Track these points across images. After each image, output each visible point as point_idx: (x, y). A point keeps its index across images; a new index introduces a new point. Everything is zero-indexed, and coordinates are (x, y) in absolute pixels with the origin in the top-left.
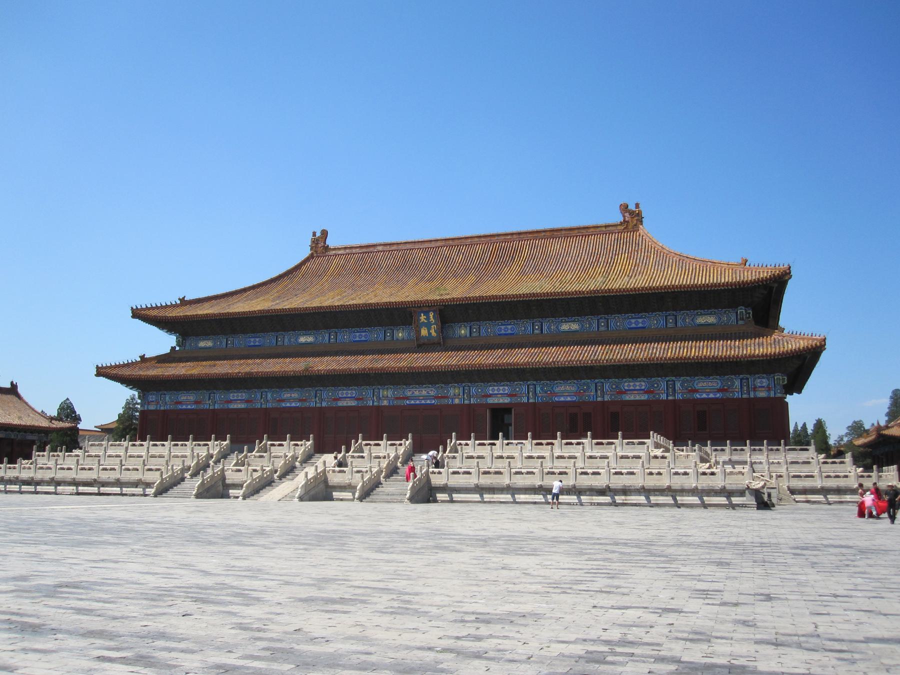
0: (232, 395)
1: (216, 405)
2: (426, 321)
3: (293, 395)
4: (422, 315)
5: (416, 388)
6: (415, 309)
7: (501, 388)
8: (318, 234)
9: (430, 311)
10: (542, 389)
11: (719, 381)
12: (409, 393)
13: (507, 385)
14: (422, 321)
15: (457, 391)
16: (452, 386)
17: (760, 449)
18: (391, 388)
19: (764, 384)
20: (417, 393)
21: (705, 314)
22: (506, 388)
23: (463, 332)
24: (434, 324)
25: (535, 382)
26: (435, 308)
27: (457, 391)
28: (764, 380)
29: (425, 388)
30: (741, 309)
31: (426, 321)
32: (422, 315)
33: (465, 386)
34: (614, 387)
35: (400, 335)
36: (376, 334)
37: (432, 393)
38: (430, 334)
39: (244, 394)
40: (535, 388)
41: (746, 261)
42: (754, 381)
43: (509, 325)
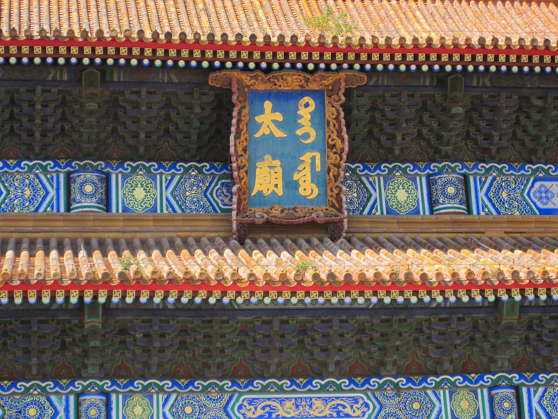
2: (279, 134)
4: (268, 105)
5: (281, 390)
6: (245, 77)
9: (302, 93)
14: (264, 131)
16: (438, 386)
18: (161, 389)
23: (401, 195)
24: (312, 147)
26: (330, 79)
27: (464, 404)
29: (323, 389)
31: (279, 134)
35: (139, 193)
36: (31, 185)
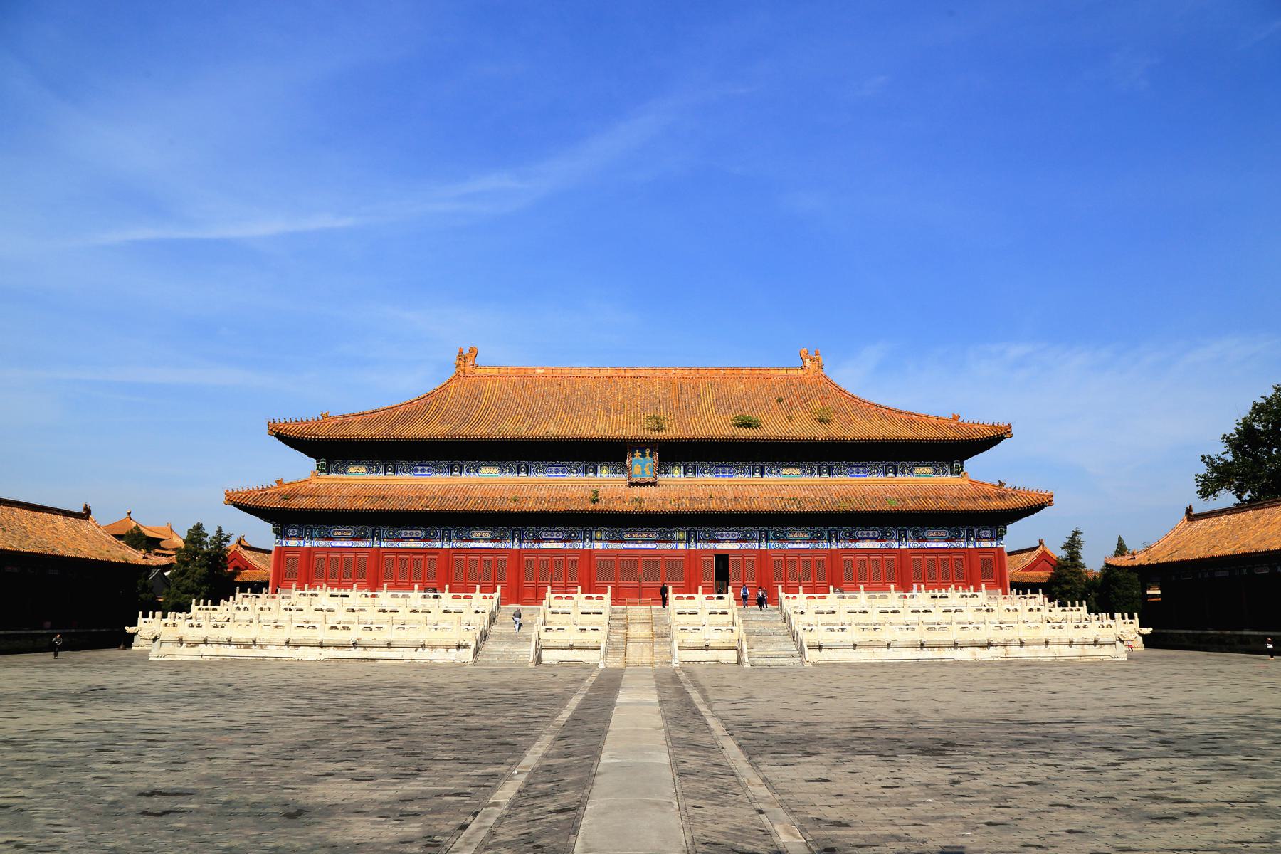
0: (403, 532)
1: (382, 543)
3: (484, 535)
4: (637, 451)
7: (731, 533)
8: (466, 352)
10: (774, 535)
11: (947, 532)
12: (626, 537)
13: (737, 531)
15: (681, 535)
17: (794, 597)
18: (605, 530)
19: (988, 536)
20: (636, 536)
21: (921, 466)
22: (736, 533)
25: (696, 529)
27: (681, 535)
28: (987, 532)
29: (646, 531)
30: (957, 462)
32: (637, 451)
33: (515, 530)
34: (707, 535)
37: (653, 537)
38: (643, 472)
39: (420, 532)
40: (591, 534)
41: (959, 417)
42: (979, 532)
43: (861, 466)
